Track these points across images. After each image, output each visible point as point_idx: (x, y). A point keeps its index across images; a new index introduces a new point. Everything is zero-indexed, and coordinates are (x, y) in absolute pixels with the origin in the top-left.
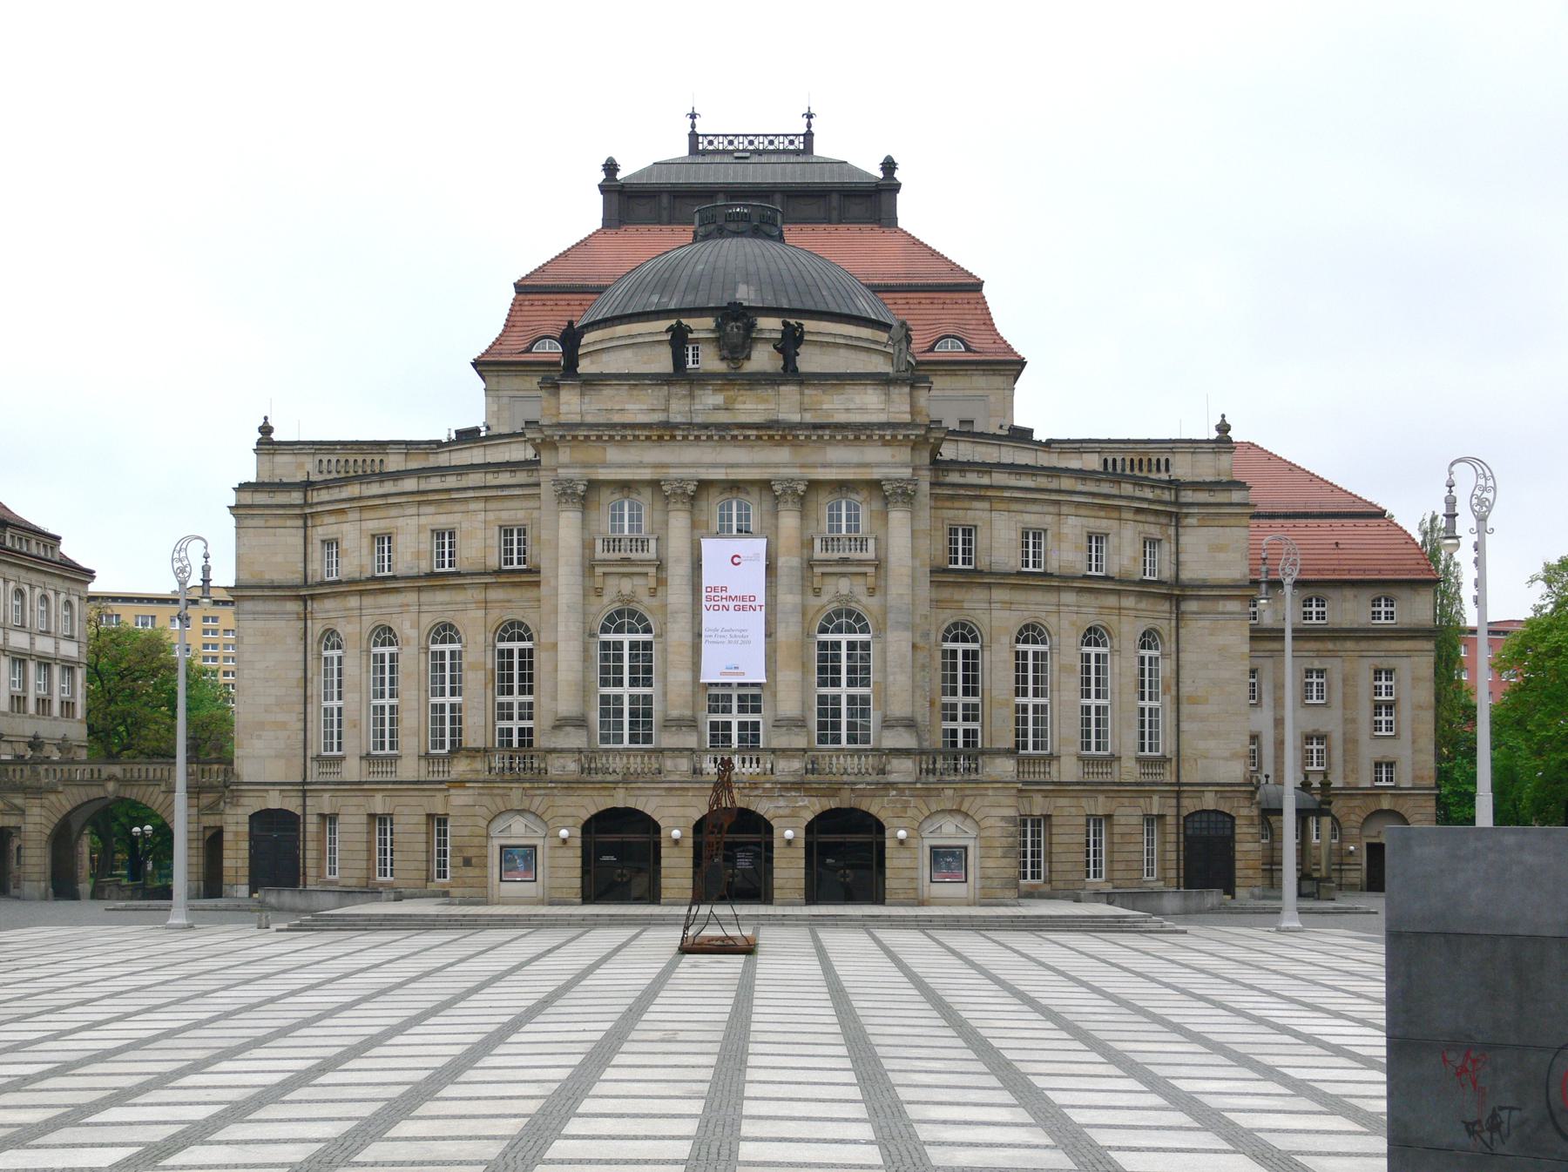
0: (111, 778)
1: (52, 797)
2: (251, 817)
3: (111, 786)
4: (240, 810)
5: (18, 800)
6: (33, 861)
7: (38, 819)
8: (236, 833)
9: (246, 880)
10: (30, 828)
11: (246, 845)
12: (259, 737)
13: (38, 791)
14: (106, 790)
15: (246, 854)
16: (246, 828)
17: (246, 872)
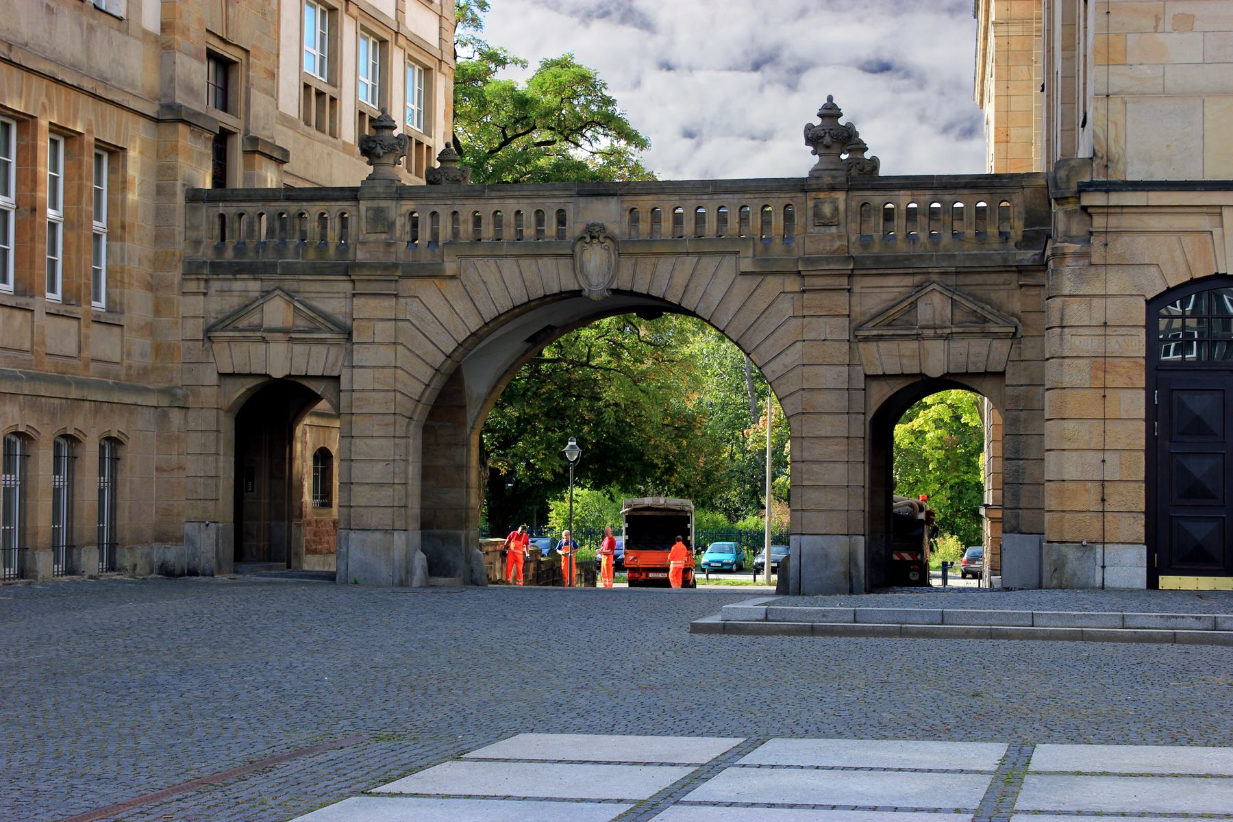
0: (593, 233)
1: (428, 292)
2: (1155, 305)
3: (595, 259)
4: (1116, 282)
5: (333, 299)
6: (376, 472)
7: (384, 355)
8: (1102, 362)
9: (1138, 528)
10: (362, 379)
11: (1133, 404)
12: (1185, 23)
13: (391, 276)
14: (578, 268)
15: (1136, 434)
16: (1137, 344)
17: (1137, 498)
